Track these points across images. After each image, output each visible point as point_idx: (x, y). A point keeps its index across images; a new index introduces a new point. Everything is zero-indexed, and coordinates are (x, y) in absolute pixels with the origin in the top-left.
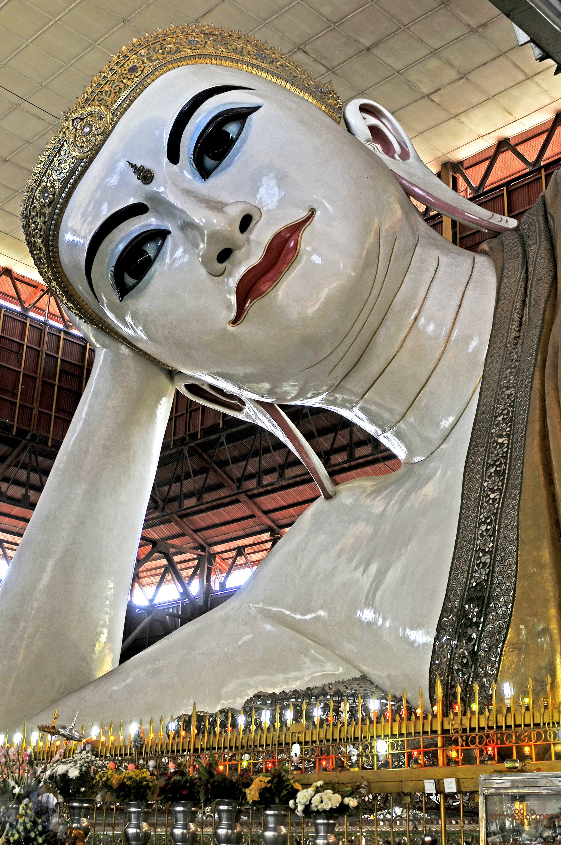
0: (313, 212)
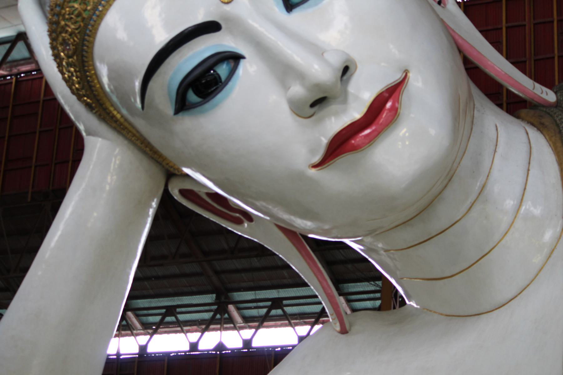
0: (406, 72)
